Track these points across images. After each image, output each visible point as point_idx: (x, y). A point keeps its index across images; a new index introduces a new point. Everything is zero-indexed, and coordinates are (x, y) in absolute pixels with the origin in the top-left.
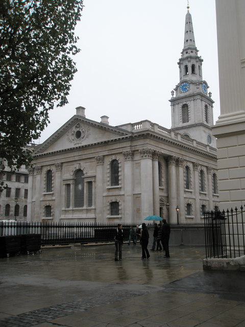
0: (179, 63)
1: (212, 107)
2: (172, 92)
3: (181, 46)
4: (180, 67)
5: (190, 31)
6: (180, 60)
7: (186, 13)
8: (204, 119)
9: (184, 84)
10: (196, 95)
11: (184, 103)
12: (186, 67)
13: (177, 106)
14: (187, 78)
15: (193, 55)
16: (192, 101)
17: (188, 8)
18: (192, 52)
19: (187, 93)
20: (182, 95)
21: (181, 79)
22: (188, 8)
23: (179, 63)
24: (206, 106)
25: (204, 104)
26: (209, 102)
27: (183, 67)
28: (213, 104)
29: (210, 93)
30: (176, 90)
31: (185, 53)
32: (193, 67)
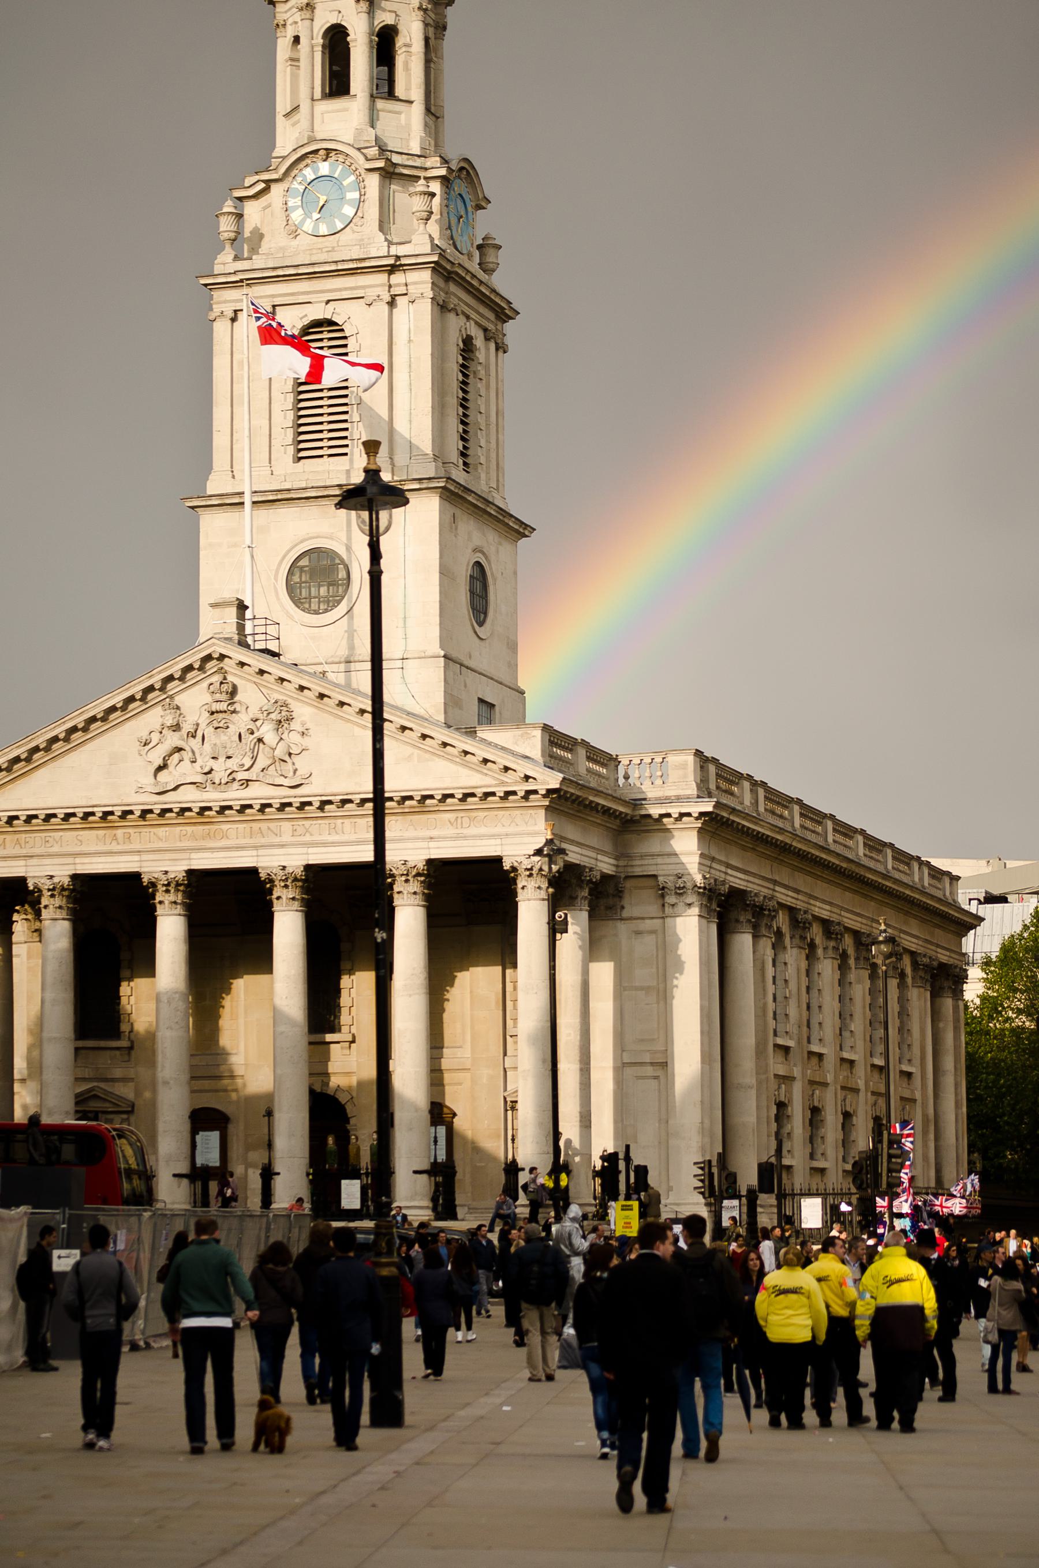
1: (501, 348)
9: (324, 168)
11: (317, 312)
24: (467, 347)
28: (509, 327)
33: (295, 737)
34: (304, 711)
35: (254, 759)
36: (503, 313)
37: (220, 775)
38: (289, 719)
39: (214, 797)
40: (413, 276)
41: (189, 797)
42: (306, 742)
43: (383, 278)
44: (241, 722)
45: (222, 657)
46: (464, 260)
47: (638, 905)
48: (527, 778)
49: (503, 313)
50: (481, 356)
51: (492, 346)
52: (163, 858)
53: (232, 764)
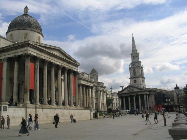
2: (130, 65)
3: (131, 49)
7: (132, 37)
11: (134, 69)
12: (134, 57)
14: (134, 60)
15: (135, 52)
16: (137, 69)
17: (133, 35)
19: (135, 66)
20: (133, 66)
21: (132, 60)
22: (133, 35)
23: (131, 55)
24: (141, 70)
25: (140, 69)
29: (142, 65)
36: (143, 68)
47: (151, 95)
49: (143, 68)
52: (128, 95)
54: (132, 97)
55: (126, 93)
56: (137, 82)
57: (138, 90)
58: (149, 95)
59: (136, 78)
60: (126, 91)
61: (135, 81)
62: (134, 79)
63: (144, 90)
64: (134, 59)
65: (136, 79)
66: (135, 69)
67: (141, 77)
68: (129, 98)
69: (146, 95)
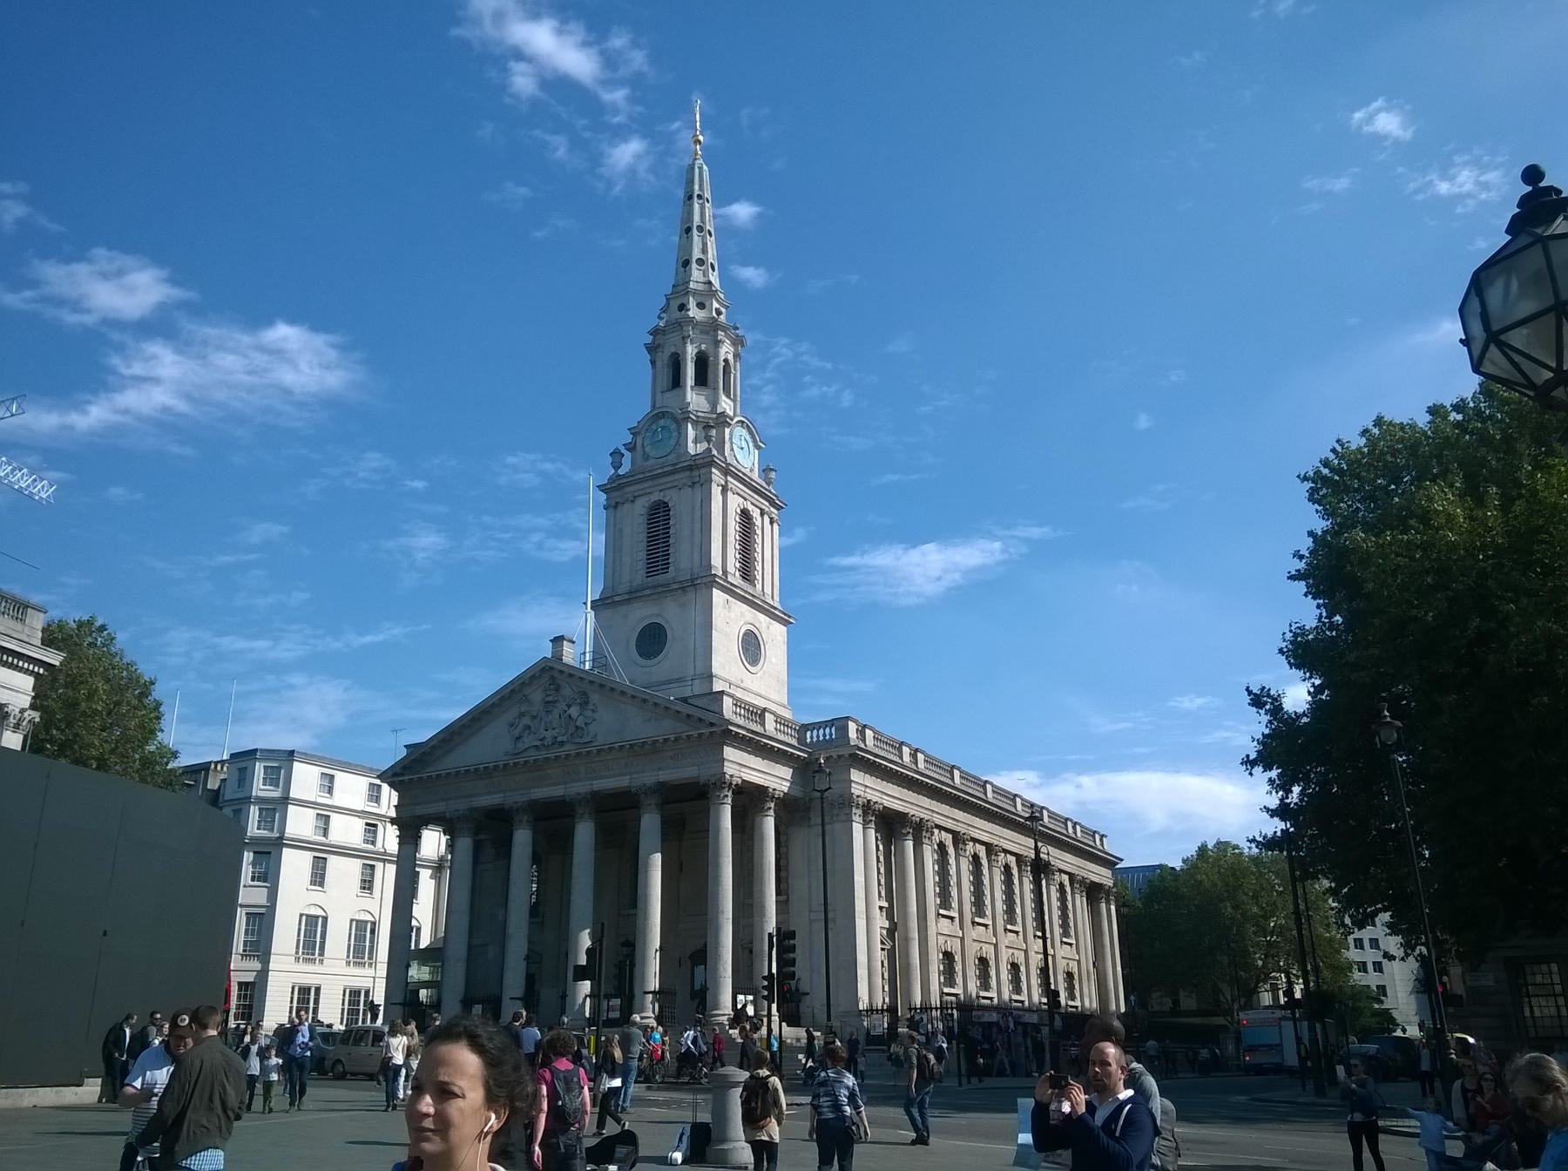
0: (652, 349)
2: (616, 454)
4: (653, 362)
5: (700, 229)
6: (655, 332)
8: (733, 564)
9: (662, 422)
10: (698, 467)
11: (656, 497)
13: (627, 506)
18: (701, 306)
24: (745, 514)
25: (735, 503)
26: (765, 504)
27: (663, 358)
30: (631, 447)
31: (675, 304)
32: (702, 363)
33: (589, 713)
34: (595, 697)
35: (567, 728)
37: (549, 740)
38: (586, 703)
39: (543, 754)
40: (703, 471)
41: (533, 755)
42: (596, 715)
43: (687, 474)
44: (561, 706)
45: (552, 668)
46: (747, 471)
48: (712, 725)
50: (758, 522)
51: (766, 519)
53: (554, 733)
54: (553, 823)
55: (485, 773)
56: (672, 648)
57: (640, 727)
58: (792, 810)
59: (660, 592)
60: (490, 747)
61: (652, 640)
62: (640, 615)
63: (705, 723)
64: (677, 381)
65: (669, 613)
66: (672, 497)
67: (729, 590)
68: (522, 838)
69: (750, 798)
